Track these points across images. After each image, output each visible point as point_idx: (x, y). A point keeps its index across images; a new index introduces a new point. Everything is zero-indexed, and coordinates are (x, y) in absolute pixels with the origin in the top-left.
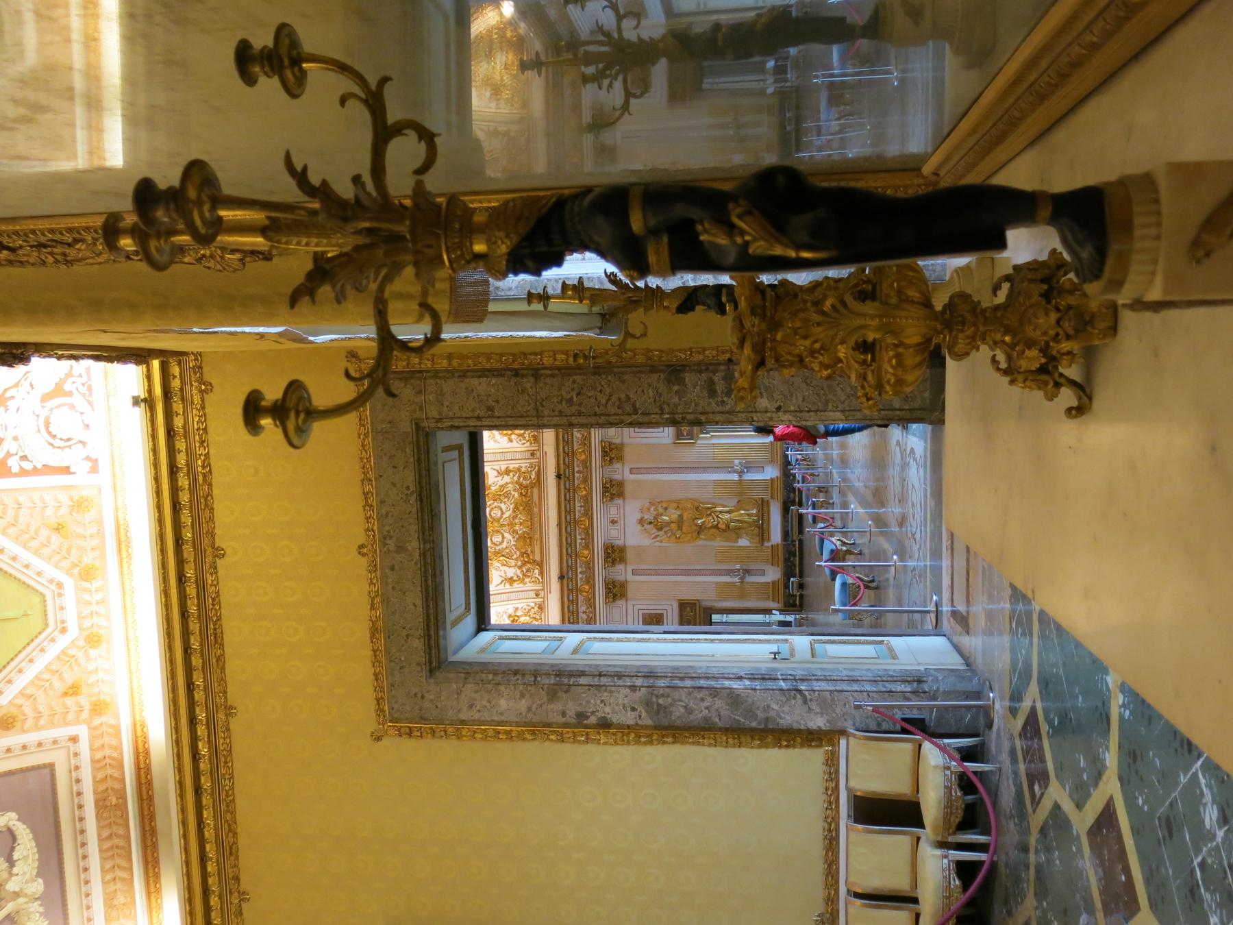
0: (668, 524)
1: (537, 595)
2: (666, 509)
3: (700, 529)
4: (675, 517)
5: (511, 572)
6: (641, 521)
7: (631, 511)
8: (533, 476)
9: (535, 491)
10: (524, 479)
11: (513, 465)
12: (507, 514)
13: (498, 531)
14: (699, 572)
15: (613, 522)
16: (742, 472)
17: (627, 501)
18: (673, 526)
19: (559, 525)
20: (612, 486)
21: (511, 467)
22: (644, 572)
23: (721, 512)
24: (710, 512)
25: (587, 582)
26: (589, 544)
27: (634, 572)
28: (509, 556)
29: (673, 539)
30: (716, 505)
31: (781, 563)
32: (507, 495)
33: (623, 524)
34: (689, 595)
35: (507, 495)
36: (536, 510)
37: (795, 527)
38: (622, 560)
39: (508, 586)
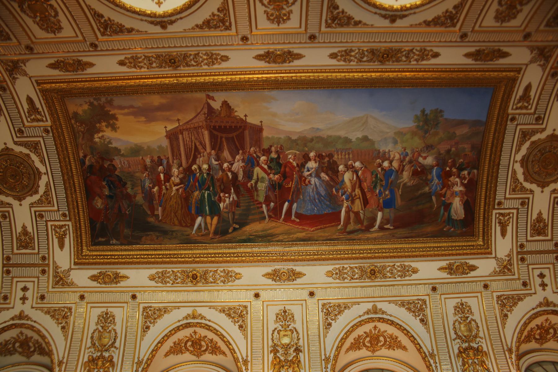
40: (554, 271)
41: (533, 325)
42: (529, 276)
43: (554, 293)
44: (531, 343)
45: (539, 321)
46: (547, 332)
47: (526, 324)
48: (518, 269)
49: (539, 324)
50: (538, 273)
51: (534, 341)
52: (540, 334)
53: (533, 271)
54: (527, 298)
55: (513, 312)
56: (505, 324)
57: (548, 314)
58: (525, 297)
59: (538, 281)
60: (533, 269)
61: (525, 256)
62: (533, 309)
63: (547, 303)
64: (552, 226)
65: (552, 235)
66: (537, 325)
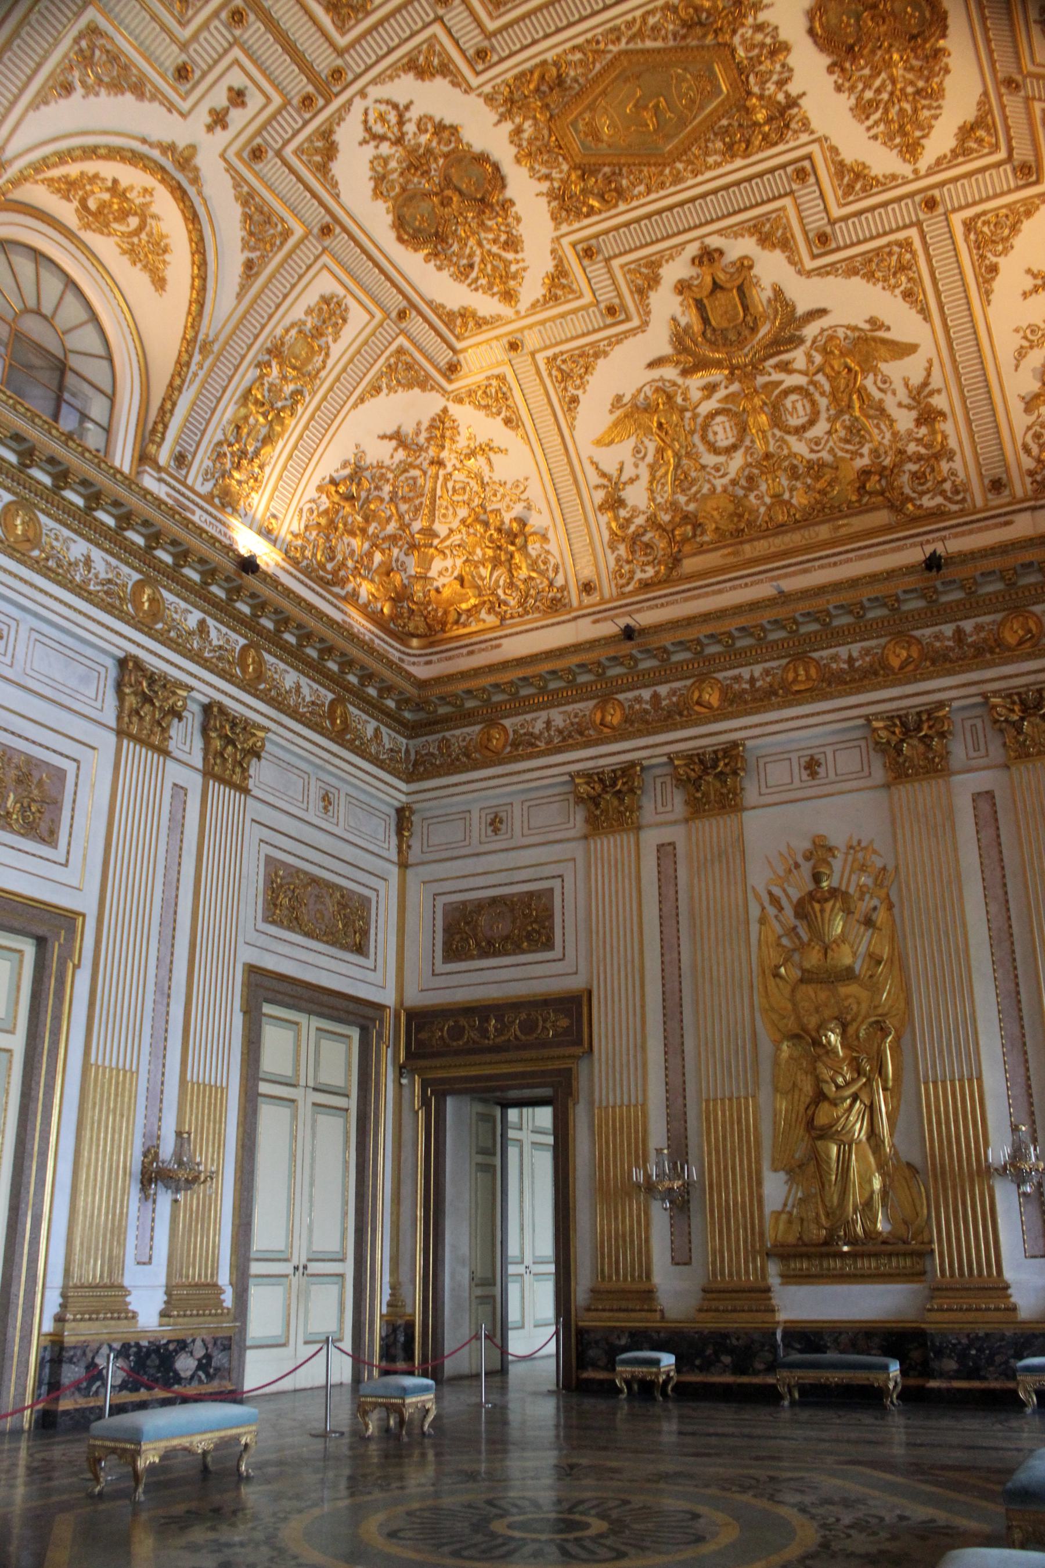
0: (817, 934)
1: (587, 588)
2: (868, 922)
3: (808, 1040)
4: (845, 957)
5: (636, 496)
6: (820, 851)
7: (849, 812)
8: (927, 502)
9: (882, 517)
10: (914, 475)
11: (952, 431)
12: (799, 447)
13: (743, 429)
14: (673, 1048)
15: (812, 766)
16: (1020, 1178)
17: (882, 794)
18: (813, 958)
19: (784, 598)
20: (926, 740)
21: (947, 427)
22: (666, 879)
23: (872, 1109)
24: (866, 1064)
25: (627, 720)
26: (736, 702)
27: (666, 851)
28: (683, 482)
29: (774, 957)
30: (894, 1092)
31: (710, 1323)
32: (855, 433)
33: (809, 790)
34: (606, 1024)
35: (855, 433)
36: (824, 531)
37: (832, 1378)
38: (697, 808)
39: (600, 496)
40: (274, 117)
41: (109, 170)
42: (211, 68)
43: (222, 156)
44: (64, 202)
45: (130, 176)
46: (123, 215)
47: (91, 152)
48: (205, 25)
49: (124, 183)
50: (236, 85)
51: (76, 204)
52: (103, 205)
53: (229, 68)
54: (156, 104)
55: (92, 98)
56: (46, 103)
57: (162, 181)
58: (153, 98)
59: (219, 98)
60: (236, 62)
61: (252, 17)
62: (144, 141)
63: (185, 160)
64: (374, 27)
65: (352, 45)
66: (115, 181)
